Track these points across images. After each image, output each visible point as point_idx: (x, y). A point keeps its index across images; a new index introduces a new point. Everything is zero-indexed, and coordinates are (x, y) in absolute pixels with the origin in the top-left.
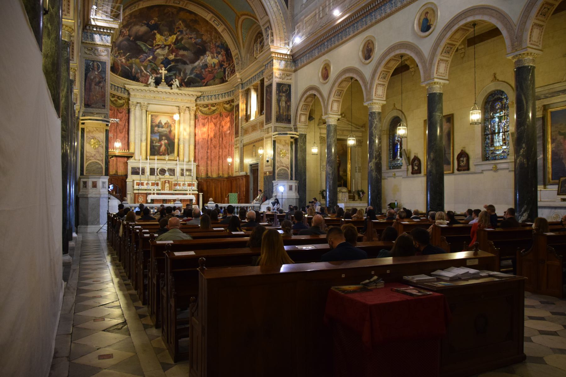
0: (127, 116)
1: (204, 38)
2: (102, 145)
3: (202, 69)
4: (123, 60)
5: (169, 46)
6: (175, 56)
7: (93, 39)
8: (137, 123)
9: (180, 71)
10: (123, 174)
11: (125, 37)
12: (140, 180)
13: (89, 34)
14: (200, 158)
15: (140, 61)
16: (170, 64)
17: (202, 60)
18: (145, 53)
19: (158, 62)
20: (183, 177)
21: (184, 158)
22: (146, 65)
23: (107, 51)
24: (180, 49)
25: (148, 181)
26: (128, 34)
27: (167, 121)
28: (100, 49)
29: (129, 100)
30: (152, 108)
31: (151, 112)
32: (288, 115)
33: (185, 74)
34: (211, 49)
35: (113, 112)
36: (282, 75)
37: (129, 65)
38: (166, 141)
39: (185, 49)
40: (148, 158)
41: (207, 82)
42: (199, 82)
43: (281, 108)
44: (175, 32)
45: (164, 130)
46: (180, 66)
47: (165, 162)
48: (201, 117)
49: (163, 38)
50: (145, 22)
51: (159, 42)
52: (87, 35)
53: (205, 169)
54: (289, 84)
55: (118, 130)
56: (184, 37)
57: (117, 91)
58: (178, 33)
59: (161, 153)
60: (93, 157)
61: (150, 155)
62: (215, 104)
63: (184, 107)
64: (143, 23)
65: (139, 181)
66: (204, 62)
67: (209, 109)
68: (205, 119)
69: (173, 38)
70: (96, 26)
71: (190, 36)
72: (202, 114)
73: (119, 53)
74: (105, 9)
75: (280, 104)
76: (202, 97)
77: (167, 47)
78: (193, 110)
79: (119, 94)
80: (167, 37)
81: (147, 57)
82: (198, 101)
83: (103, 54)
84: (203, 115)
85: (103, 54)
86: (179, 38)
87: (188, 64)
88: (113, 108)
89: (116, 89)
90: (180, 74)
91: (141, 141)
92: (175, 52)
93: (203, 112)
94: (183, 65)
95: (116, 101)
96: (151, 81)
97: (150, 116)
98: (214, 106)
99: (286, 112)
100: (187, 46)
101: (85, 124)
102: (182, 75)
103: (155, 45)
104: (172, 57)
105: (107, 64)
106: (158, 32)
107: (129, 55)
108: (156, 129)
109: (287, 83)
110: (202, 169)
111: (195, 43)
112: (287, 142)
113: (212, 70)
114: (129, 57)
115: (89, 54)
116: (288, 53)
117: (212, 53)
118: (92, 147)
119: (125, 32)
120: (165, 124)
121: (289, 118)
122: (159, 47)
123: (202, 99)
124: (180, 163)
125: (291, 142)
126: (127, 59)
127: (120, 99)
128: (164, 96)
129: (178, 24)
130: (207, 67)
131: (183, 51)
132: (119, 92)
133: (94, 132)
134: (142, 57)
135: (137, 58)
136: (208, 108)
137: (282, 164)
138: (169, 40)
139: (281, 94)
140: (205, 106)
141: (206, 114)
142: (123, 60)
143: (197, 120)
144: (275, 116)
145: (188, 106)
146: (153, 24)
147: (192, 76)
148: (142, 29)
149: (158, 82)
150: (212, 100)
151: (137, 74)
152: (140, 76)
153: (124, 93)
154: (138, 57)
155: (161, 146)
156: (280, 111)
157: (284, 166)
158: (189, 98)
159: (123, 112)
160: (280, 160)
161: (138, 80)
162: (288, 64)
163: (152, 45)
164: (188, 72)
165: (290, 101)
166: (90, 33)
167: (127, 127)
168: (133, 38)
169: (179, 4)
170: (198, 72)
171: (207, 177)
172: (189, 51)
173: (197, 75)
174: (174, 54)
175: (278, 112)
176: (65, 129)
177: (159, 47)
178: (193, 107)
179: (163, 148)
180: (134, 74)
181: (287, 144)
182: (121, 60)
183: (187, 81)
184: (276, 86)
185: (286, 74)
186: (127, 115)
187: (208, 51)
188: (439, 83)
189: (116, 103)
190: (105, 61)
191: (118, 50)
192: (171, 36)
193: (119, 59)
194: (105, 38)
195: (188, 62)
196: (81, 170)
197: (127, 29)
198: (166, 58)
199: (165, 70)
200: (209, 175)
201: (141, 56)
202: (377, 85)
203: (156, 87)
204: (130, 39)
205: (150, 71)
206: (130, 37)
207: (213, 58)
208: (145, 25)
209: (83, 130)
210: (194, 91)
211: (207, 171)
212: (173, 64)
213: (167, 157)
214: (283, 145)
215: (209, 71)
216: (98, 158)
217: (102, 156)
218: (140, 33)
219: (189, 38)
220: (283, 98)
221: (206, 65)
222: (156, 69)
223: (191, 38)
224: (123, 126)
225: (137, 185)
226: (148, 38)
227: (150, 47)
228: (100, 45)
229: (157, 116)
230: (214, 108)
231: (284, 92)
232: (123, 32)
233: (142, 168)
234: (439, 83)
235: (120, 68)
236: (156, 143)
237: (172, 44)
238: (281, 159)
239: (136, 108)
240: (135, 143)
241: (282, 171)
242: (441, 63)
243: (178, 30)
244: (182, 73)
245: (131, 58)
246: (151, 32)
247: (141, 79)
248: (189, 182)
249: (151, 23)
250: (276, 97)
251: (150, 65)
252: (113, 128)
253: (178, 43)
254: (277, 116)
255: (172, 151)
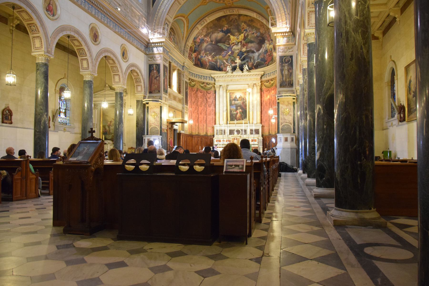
0: (214, 95)
1: (261, 31)
2: (158, 116)
3: (264, 54)
4: (210, 58)
5: (241, 42)
6: (246, 49)
7: (153, 51)
8: (221, 99)
9: (250, 58)
10: (211, 135)
11: (208, 43)
12: (228, 139)
13: (151, 48)
14: (265, 120)
15: (223, 57)
16: (243, 55)
17: (264, 48)
18: (225, 50)
19: (235, 55)
20: (217, 135)
21: (253, 121)
22: (227, 58)
23: (161, 56)
24: (249, 43)
25: (223, 138)
26: (210, 40)
27: (241, 96)
28: (157, 56)
29: (215, 84)
30: (230, 88)
31: (230, 91)
32: (290, 81)
33: (254, 61)
34: (267, 38)
35: (203, 94)
36: (285, 49)
37: (214, 61)
38: (241, 110)
39: (251, 42)
40: (228, 123)
41: (268, 63)
42: (263, 64)
43: (284, 75)
44: (242, 32)
45: (239, 102)
46: (251, 55)
47: (234, 125)
48: (265, 90)
49: (235, 37)
50: (220, 30)
51: (233, 41)
52: (150, 49)
53: (268, 128)
54: (291, 55)
55: (207, 105)
56: (249, 33)
57: (206, 79)
58: (244, 32)
59: (238, 119)
60: (153, 124)
61: (230, 121)
62: (273, 78)
63: (252, 84)
64: (218, 31)
65: (217, 139)
66: (265, 49)
67: (270, 83)
68: (267, 91)
69: (242, 36)
70: (154, 43)
71: (252, 32)
72: (265, 88)
73: (205, 54)
74: (159, 31)
75: (283, 73)
76: (265, 75)
77: (240, 43)
78: (217, 87)
79: (207, 81)
80: (238, 36)
81: (227, 53)
82: (263, 78)
83: (158, 59)
84: (267, 88)
85: (158, 59)
86: (246, 35)
87: (255, 53)
88: (203, 91)
89: (205, 78)
90: (251, 60)
91: (223, 111)
92: (245, 46)
93: (266, 86)
94: (252, 54)
95: (206, 86)
96: (229, 69)
97: (229, 93)
98: (272, 81)
99: (288, 79)
100: (252, 39)
101: (149, 104)
102: (252, 61)
103: (232, 44)
104: (244, 50)
105: (161, 65)
106: (231, 34)
107: (214, 54)
108: (233, 102)
109: (289, 55)
110: (266, 128)
111: (257, 36)
112: (290, 102)
113: (271, 54)
114: (214, 56)
115: (151, 61)
116: (288, 30)
117: (269, 41)
118: (153, 117)
119: (207, 39)
120: (239, 98)
121: (291, 83)
122: (234, 44)
123: (265, 77)
124: (250, 125)
125: (294, 103)
126: (213, 57)
127: (208, 85)
128: (237, 78)
129: (242, 25)
130: (268, 52)
131: (251, 43)
132: (208, 80)
133: (154, 108)
134: (223, 54)
135: (220, 55)
136: (269, 83)
137: (285, 121)
138: (240, 38)
139: (284, 65)
140: (267, 81)
141: (268, 87)
142: (210, 58)
143: (262, 93)
144: (279, 83)
145: (255, 83)
146: (226, 30)
147: (259, 60)
148: (219, 35)
149: (234, 69)
150: (266, 77)
151: (221, 66)
152: (223, 67)
153: (212, 80)
154: (221, 54)
155: (237, 113)
156: (283, 79)
157: (287, 122)
158: (256, 77)
159: (211, 93)
160: (284, 118)
161: (222, 69)
162: (290, 39)
163: (229, 44)
164: (256, 57)
165: (293, 69)
166: (152, 48)
167: (214, 103)
168: (214, 42)
169: (233, 12)
170: (262, 57)
171: (269, 135)
172: (255, 43)
173: (262, 60)
174: (245, 47)
175: (282, 79)
176: (42, 109)
177: (234, 44)
178: (258, 84)
179: (238, 115)
180: (218, 66)
181: (290, 104)
182: (208, 58)
183: (256, 65)
184: (279, 59)
185: (288, 48)
186: (214, 95)
187: (266, 40)
188: (312, 34)
189: (205, 87)
190: (159, 63)
191: (205, 52)
192: (240, 35)
193: (207, 58)
194: (159, 49)
195: (255, 51)
196: (147, 132)
197: (208, 38)
198: (241, 51)
199: (239, 60)
200: (271, 133)
201: (223, 53)
202: (303, 45)
203: (243, 72)
204: (212, 44)
205: (231, 62)
206: (212, 42)
207: (270, 44)
208: (220, 32)
209: (148, 107)
210: (259, 72)
211: (269, 130)
212: (245, 54)
213: (243, 121)
214: (286, 106)
215: (269, 55)
216: (156, 124)
217: (158, 123)
218: (219, 38)
219: (252, 34)
220: (286, 68)
221: (267, 51)
222: (234, 60)
223: (253, 33)
224: (211, 103)
225: (217, 141)
226: (225, 40)
227: (228, 46)
228: (157, 54)
229: (233, 93)
230: (272, 82)
231: (286, 63)
232: (206, 40)
233: (244, 130)
234: (312, 34)
235: (208, 64)
236: (234, 112)
237: (243, 40)
238: (285, 117)
239: (220, 89)
240: (219, 113)
241: (285, 126)
242: (311, 14)
243: (244, 29)
244: (252, 60)
245: (216, 56)
246: (226, 35)
247: (224, 69)
248: (252, 139)
249: (224, 29)
250: (279, 68)
251: (230, 58)
252: (203, 104)
253: (246, 39)
254: (280, 83)
255: (245, 117)
